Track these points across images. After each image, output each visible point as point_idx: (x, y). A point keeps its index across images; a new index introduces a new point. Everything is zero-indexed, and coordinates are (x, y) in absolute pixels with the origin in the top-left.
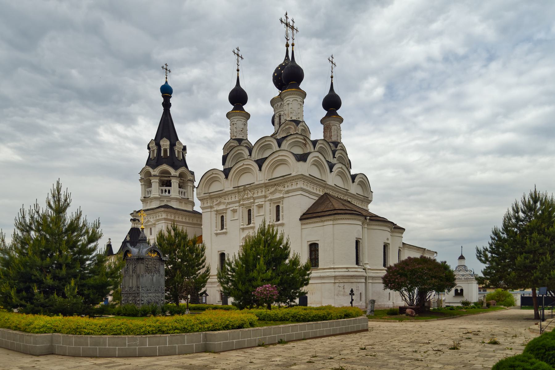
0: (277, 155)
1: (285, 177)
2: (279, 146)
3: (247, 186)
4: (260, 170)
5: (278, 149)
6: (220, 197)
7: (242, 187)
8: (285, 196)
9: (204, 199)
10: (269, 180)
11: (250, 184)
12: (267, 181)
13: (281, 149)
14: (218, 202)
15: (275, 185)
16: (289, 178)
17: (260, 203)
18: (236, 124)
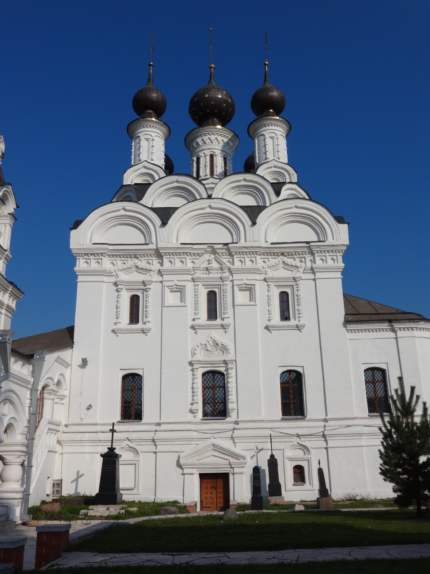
0: (294, 205)
1: (311, 244)
2: (278, 193)
3: (216, 246)
4: (254, 223)
5: (274, 198)
6: (136, 257)
7: (205, 246)
8: (304, 276)
9: (91, 254)
10: (272, 244)
11: (226, 244)
12: (268, 245)
13: (281, 197)
14: (125, 266)
15: (283, 254)
16: (319, 246)
17: (247, 282)
18: (153, 140)
